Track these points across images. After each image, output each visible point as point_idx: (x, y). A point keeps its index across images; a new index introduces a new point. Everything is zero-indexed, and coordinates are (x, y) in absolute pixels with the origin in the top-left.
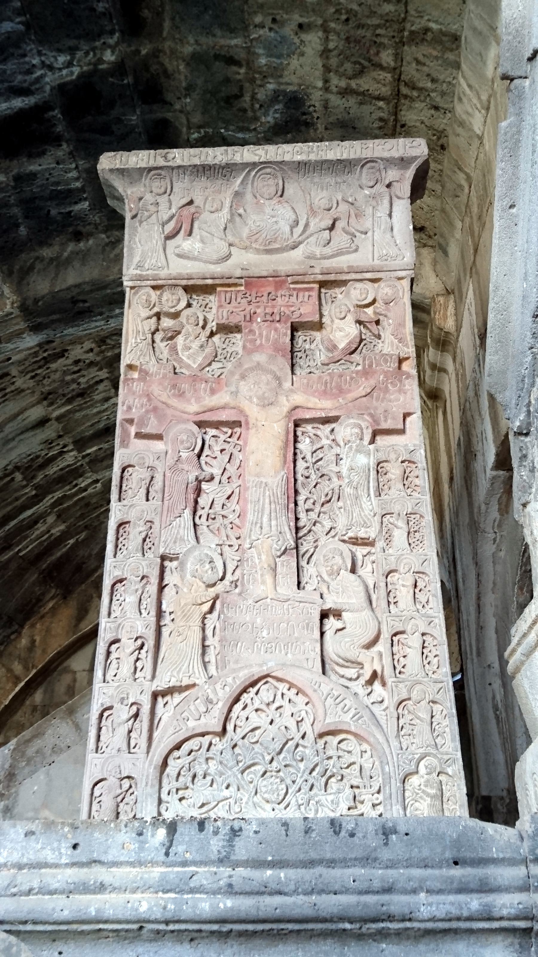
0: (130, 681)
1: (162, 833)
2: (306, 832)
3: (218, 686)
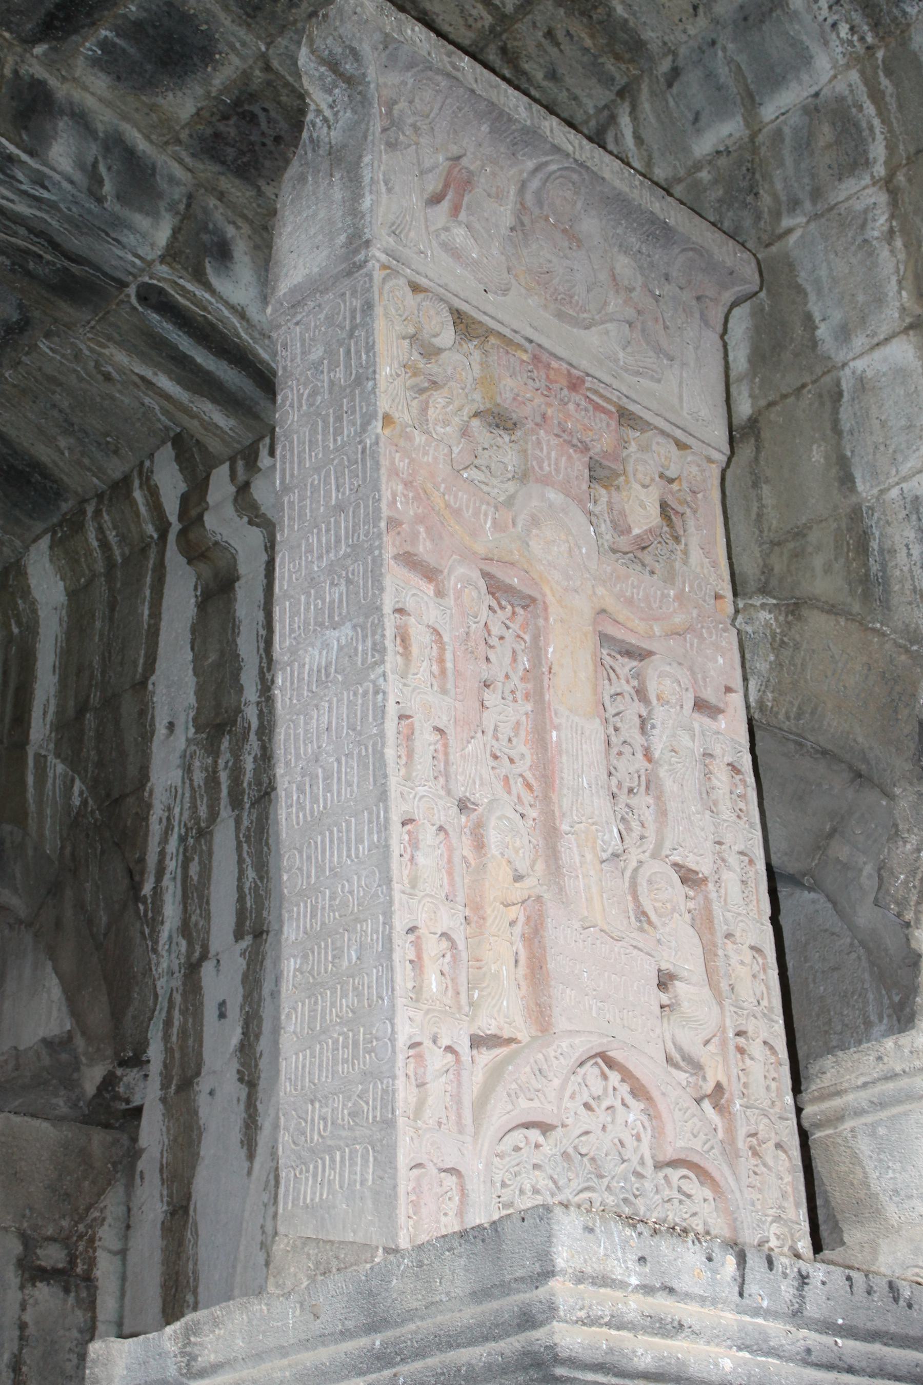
1: (731, 1261)
2: (869, 1293)
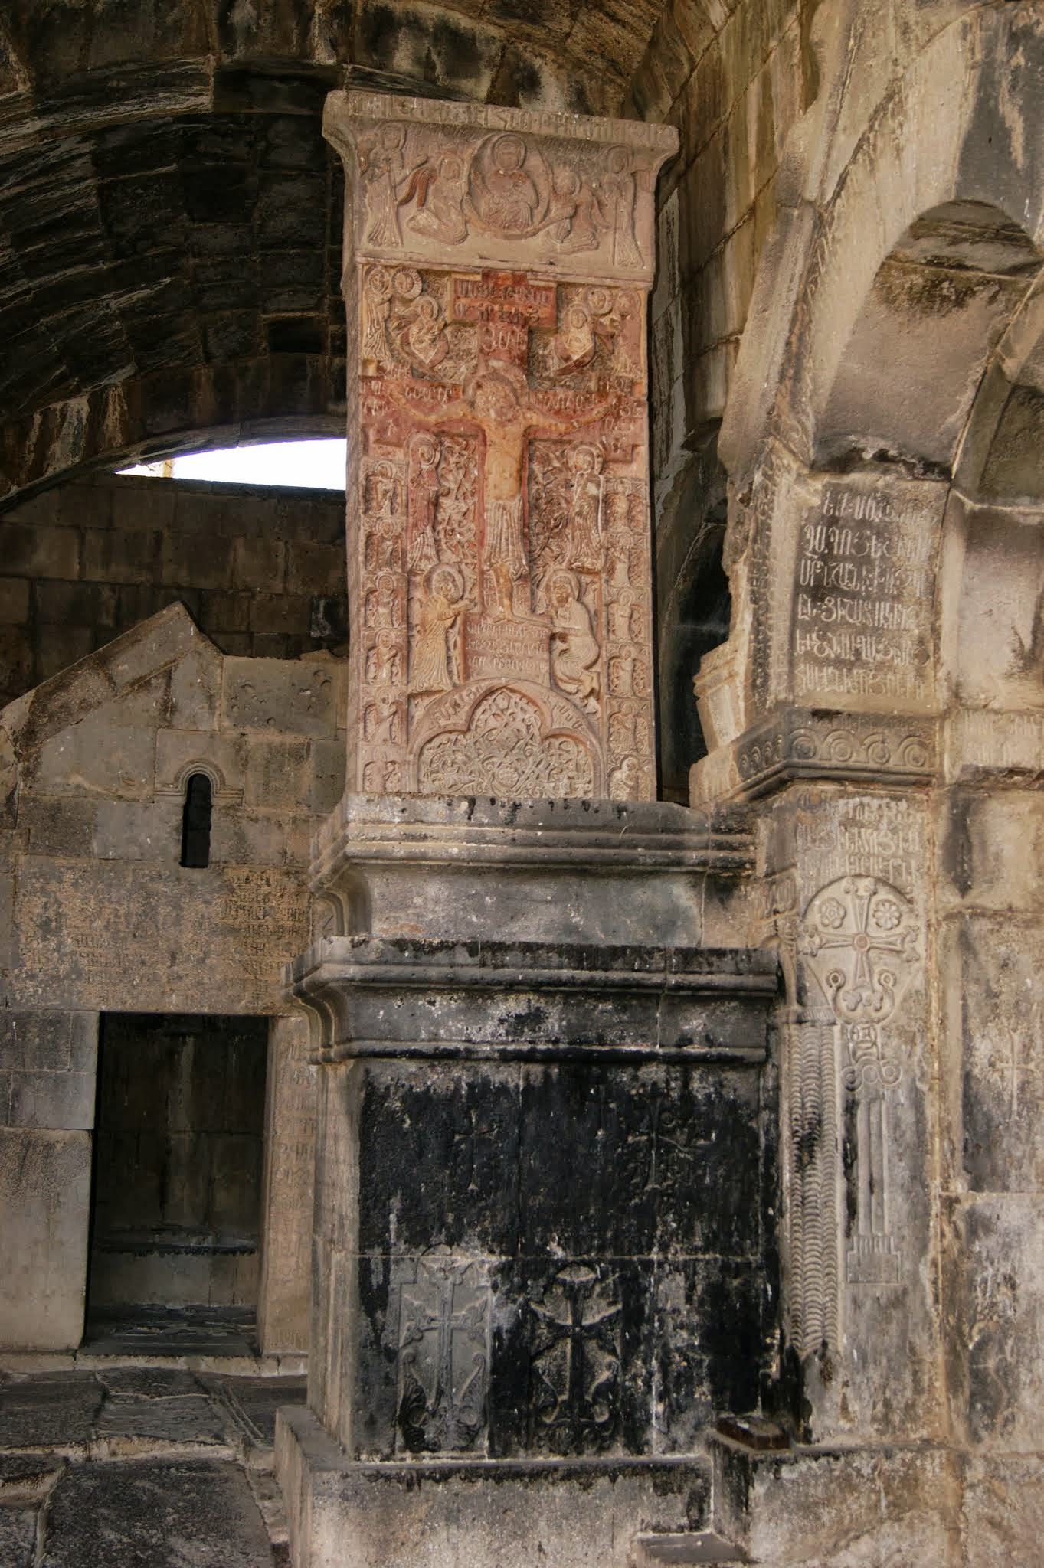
0: (388, 683)
1: (465, 805)
3: (464, 693)
